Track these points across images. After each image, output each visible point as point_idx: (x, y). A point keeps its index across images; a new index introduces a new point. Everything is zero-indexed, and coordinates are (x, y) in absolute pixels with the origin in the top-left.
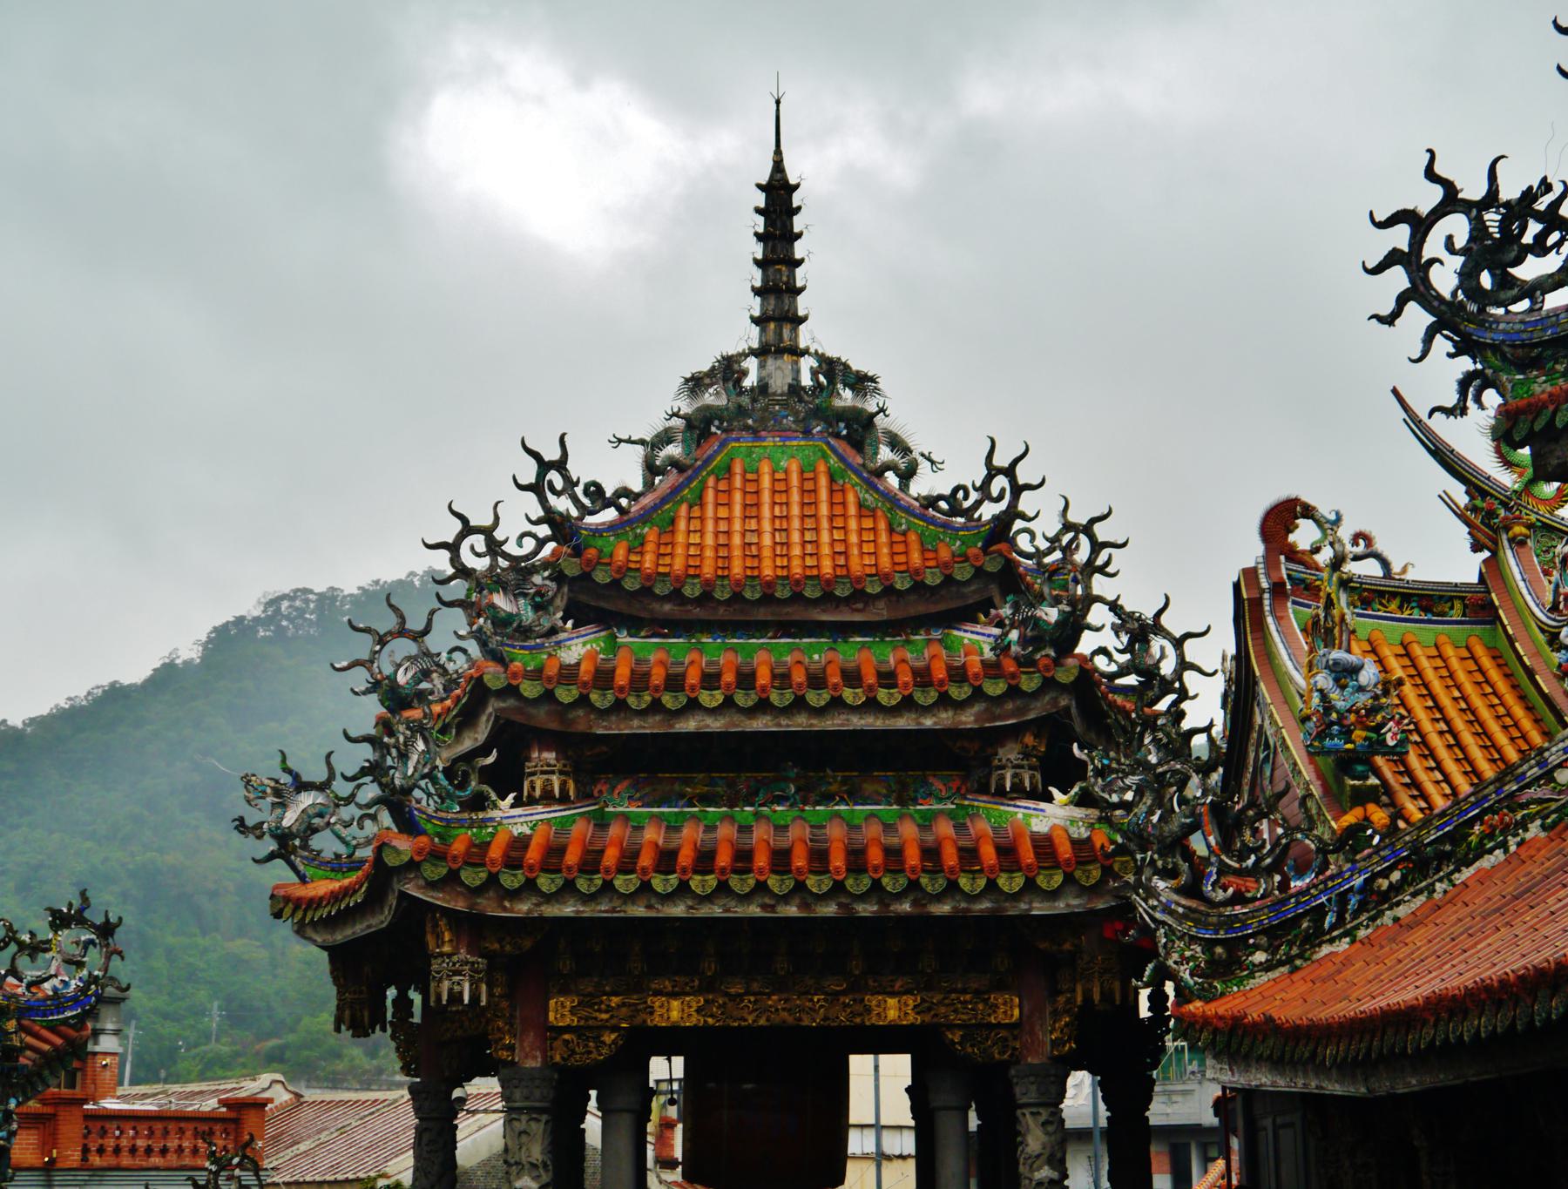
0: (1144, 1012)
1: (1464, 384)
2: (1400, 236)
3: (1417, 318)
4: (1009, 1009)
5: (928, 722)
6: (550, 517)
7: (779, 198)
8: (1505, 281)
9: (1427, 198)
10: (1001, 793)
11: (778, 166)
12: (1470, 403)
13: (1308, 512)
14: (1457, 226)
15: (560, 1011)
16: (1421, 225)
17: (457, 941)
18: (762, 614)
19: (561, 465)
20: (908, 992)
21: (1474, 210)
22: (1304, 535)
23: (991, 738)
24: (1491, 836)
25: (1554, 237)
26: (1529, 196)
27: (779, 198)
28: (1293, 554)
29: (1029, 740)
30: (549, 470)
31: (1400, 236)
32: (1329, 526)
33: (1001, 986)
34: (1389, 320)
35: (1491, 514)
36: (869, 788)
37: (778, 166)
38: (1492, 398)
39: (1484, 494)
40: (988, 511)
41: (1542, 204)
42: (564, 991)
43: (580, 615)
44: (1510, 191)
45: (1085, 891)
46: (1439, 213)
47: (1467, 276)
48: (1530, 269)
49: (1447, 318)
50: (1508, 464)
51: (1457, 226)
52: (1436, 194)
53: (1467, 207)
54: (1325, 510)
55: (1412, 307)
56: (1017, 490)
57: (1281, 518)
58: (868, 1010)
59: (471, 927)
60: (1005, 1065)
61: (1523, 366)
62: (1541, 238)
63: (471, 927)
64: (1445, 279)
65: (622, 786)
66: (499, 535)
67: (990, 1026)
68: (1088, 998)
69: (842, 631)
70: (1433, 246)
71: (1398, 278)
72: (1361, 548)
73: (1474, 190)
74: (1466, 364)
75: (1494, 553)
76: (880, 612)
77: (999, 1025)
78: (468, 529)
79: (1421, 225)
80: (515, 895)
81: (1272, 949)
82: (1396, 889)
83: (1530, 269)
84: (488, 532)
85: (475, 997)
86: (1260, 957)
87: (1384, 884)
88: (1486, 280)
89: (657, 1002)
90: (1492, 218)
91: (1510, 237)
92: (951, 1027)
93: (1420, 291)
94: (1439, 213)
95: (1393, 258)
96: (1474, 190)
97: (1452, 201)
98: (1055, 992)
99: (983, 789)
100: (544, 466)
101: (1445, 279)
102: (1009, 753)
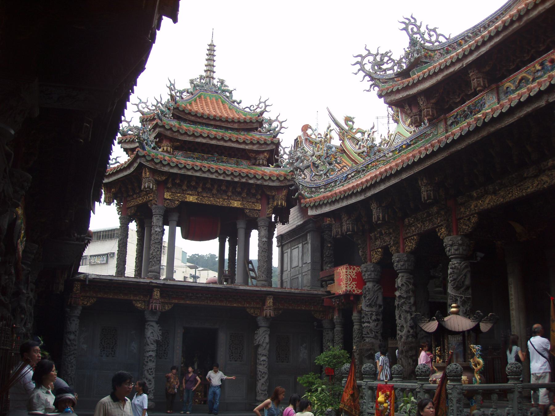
0: (273, 220)
1: (371, 86)
2: (359, 59)
3: (362, 74)
4: (259, 207)
5: (247, 147)
7: (211, 49)
8: (380, 68)
9: (365, 53)
10: (259, 165)
12: (372, 89)
13: (310, 128)
14: (371, 58)
15: (167, 195)
16: (363, 58)
18: (212, 123)
20: (239, 201)
22: (309, 132)
23: (258, 152)
24: (373, 167)
25: (390, 61)
26: (387, 53)
27: (211, 49)
28: (308, 135)
29: (266, 154)
31: (359, 59)
33: (257, 202)
34: (356, 74)
35: (343, 134)
36: (230, 161)
38: (377, 89)
39: (343, 129)
40: (259, 110)
41: (389, 55)
42: (168, 191)
44: (382, 51)
45: (280, 181)
46: (366, 56)
47: (373, 68)
48: (384, 67)
49: (368, 74)
50: (347, 125)
51: (371, 58)
52: (367, 52)
53: (372, 55)
54: (314, 128)
55: (361, 72)
56: (266, 106)
57: (305, 128)
58: (231, 203)
59: (154, 172)
60: (257, 218)
61: (383, 83)
62: (388, 61)
63: (154, 172)
64: (368, 67)
65: (180, 153)
66: (148, 104)
67: (255, 210)
68: (277, 204)
69: (227, 129)
70: (365, 61)
71: (358, 67)
72: (319, 136)
73: (374, 52)
74: (371, 83)
75: (343, 141)
77: (257, 210)
78: (141, 102)
79: (363, 58)
80: (164, 166)
81: (325, 189)
82: (352, 177)
83: (384, 67)
84: (145, 103)
85: (153, 188)
86: (323, 190)
87: (350, 176)
88: (376, 68)
89: (188, 196)
90: (378, 58)
91: (382, 60)
92: (247, 209)
93: (362, 69)
94: (366, 56)
95: (357, 63)
96: (374, 52)
97: (369, 54)
98: (268, 204)
99: (254, 164)
101: (368, 67)
102: (262, 156)
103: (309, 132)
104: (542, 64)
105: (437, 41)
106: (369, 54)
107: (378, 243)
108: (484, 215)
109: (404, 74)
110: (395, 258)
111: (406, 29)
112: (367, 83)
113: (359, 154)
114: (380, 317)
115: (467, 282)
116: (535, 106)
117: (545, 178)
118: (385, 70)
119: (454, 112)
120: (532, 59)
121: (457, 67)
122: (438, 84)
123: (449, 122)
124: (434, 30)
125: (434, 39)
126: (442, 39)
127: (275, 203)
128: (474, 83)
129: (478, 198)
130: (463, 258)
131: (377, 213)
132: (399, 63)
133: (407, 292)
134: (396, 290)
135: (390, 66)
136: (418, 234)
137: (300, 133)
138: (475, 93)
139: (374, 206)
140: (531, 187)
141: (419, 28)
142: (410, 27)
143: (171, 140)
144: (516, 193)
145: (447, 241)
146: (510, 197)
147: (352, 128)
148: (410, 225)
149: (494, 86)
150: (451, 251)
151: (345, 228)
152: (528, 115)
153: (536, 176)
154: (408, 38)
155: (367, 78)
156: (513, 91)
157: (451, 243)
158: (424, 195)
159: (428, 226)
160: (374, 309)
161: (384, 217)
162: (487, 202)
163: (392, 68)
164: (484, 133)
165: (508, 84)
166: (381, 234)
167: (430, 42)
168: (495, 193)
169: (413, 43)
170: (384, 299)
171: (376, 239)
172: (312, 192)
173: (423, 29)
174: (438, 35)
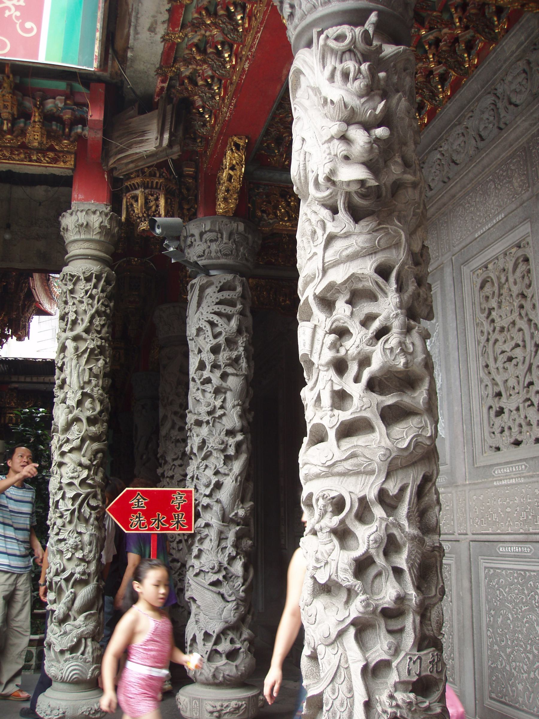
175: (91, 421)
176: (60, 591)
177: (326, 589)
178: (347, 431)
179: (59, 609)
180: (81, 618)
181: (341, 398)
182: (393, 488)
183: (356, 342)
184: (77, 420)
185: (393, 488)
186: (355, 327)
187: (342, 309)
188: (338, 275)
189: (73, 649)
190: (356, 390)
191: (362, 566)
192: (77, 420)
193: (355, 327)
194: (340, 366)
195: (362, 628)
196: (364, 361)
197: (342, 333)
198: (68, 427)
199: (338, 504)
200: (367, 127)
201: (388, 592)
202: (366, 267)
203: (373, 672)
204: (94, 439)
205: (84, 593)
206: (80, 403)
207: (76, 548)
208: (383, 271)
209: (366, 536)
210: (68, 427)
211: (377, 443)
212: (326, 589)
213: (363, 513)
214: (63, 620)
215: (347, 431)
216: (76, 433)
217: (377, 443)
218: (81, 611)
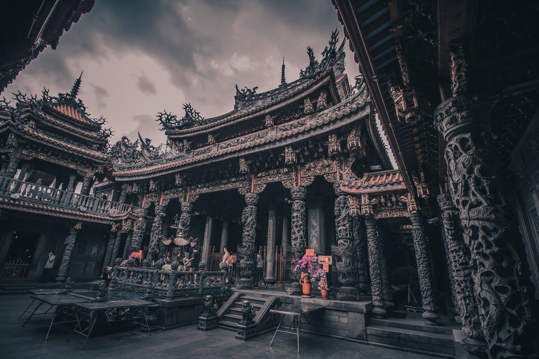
6: (44, 97)
9: (164, 113)
11: (80, 78)
17: (14, 138)
19: (47, 93)
21: (168, 116)
22: (126, 141)
30: (46, 92)
31: (160, 115)
32: (128, 141)
36: (75, 143)
37: (80, 78)
38: (165, 130)
40: (99, 122)
43: (43, 110)
47: (166, 120)
48: (171, 122)
49: (162, 122)
51: (166, 116)
57: (124, 138)
64: (164, 120)
71: (159, 118)
76: (83, 126)
78: (20, 94)
79: (162, 115)
83: (171, 122)
90: (169, 117)
93: (161, 119)
97: (166, 114)
98: (93, 170)
100: (45, 91)
101: (164, 120)
102: (95, 146)
103: (126, 141)
104: (238, 140)
105: (198, 118)
106: (166, 114)
107: (149, 200)
108: (201, 195)
109: (180, 128)
110: (156, 208)
111: (185, 109)
112: (161, 126)
113: (149, 157)
114: (142, 235)
115: (188, 224)
116: (233, 156)
117: (230, 185)
118: (172, 123)
119: (198, 150)
120: (235, 137)
121: (204, 131)
122: (194, 136)
123: (195, 154)
124: (198, 113)
125: (196, 117)
126: (200, 118)
127: (97, 171)
128: (210, 140)
129: (200, 188)
130: (189, 212)
131: (152, 186)
132: (179, 122)
133: (159, 224)
134: (153, 223)
135: (174, 122)
136: (170, 199)
137: (121, 140)
138: (209, 145)
139: (151, 182)
140: (224, 188)
141: (191, 110)
142: (188, 108)
143: (37, 122)
144: (217, 189)
145: (183, 204)
146: (214, 190)
147: (149, 145)
148: (167, 194)
149: (217, 144)
150: (184, 209)
151: (134, 190)
152: (229, 159)
153: (227, 184)
154: (185, 113)
155: (162, 124)
156: (224, 148)
157: (185, 205)
158: (177, 182)
159: (176, 196)
160: (140, 231)
161: (155, 188)
162: (205, 190)
163: (175, 124)
164: (210, 162)
165: (223, 144)
166: (152, 196)
167: (195, 118)
168: (208, 187)
169: (187, 115)
170: (147, 226)
171: (149, 198)
172: (120, 170)
173: (193, 111)
174: (199, 116)
175: (424, 258)
176: (424, 292)
177: (459, 292)
178: (458, 271)
179: (424, 295)
180: (429, 298)
181: (456, 266)
182: (466, 279)
183: (457, 259)
184: (421, 258)
185: (466, 279)
186: (456, 256)
187: (454, 254)
188: (453, 249)
189: (428, 304)
190: (458, 265)
191: (463, 290)
192: (421, 258)
193: (456, 256)
194: (455, 261)
195: (465, 298)
196: (459, 261)
197: (454, 257)
198: (419, 259)
199: (457, 281)
200: (451, 230)
201: (467, 294)
202: (457, 248)
203: (467, 305)
204: (425, 261)
205: (429, 292)
206: (421, 254)
207: (425, 283)
208: (460, 248)
209: (462, 285)
210: (419, 259)
211: (462, 273)
212: (459, 292)
213: (462, 282)
214: (425, 298)
215: (458, 271)
216: (421, 260)
217: (462, 273)
218: (429, 296)
